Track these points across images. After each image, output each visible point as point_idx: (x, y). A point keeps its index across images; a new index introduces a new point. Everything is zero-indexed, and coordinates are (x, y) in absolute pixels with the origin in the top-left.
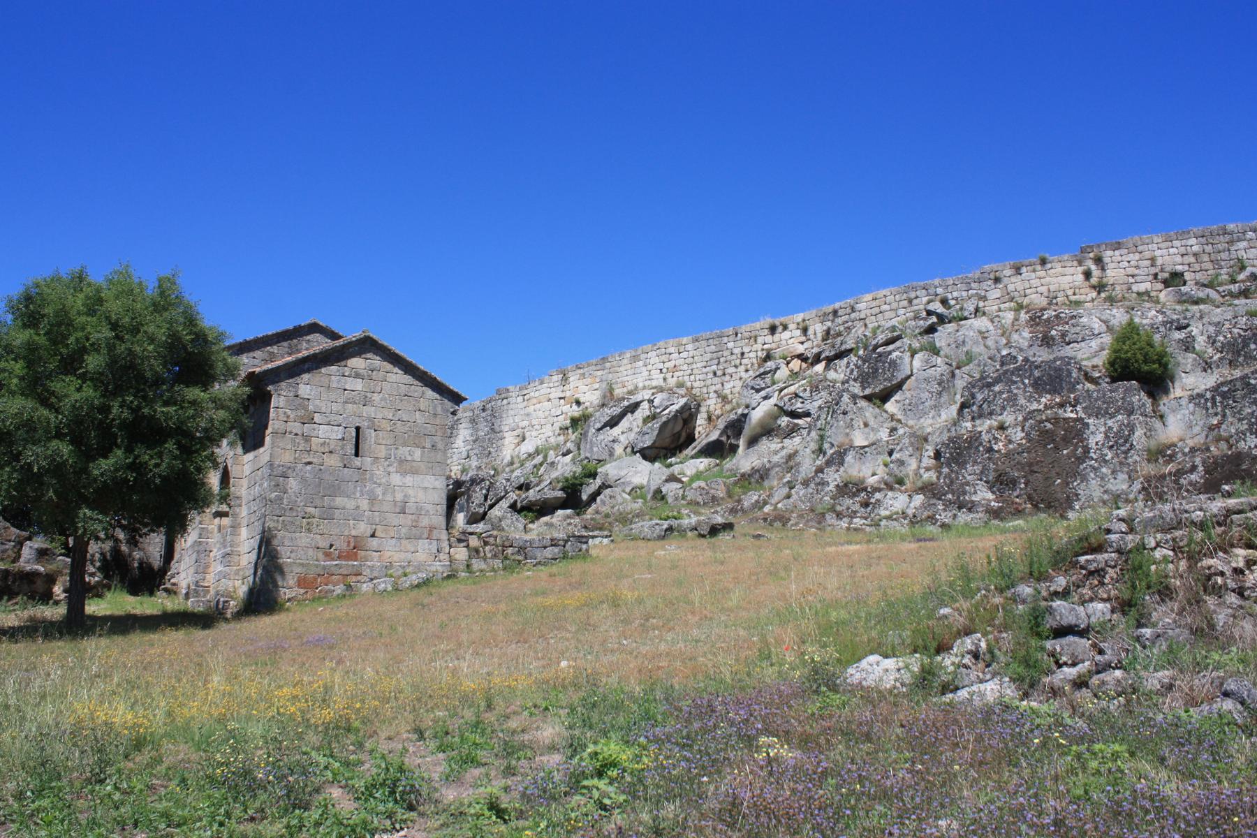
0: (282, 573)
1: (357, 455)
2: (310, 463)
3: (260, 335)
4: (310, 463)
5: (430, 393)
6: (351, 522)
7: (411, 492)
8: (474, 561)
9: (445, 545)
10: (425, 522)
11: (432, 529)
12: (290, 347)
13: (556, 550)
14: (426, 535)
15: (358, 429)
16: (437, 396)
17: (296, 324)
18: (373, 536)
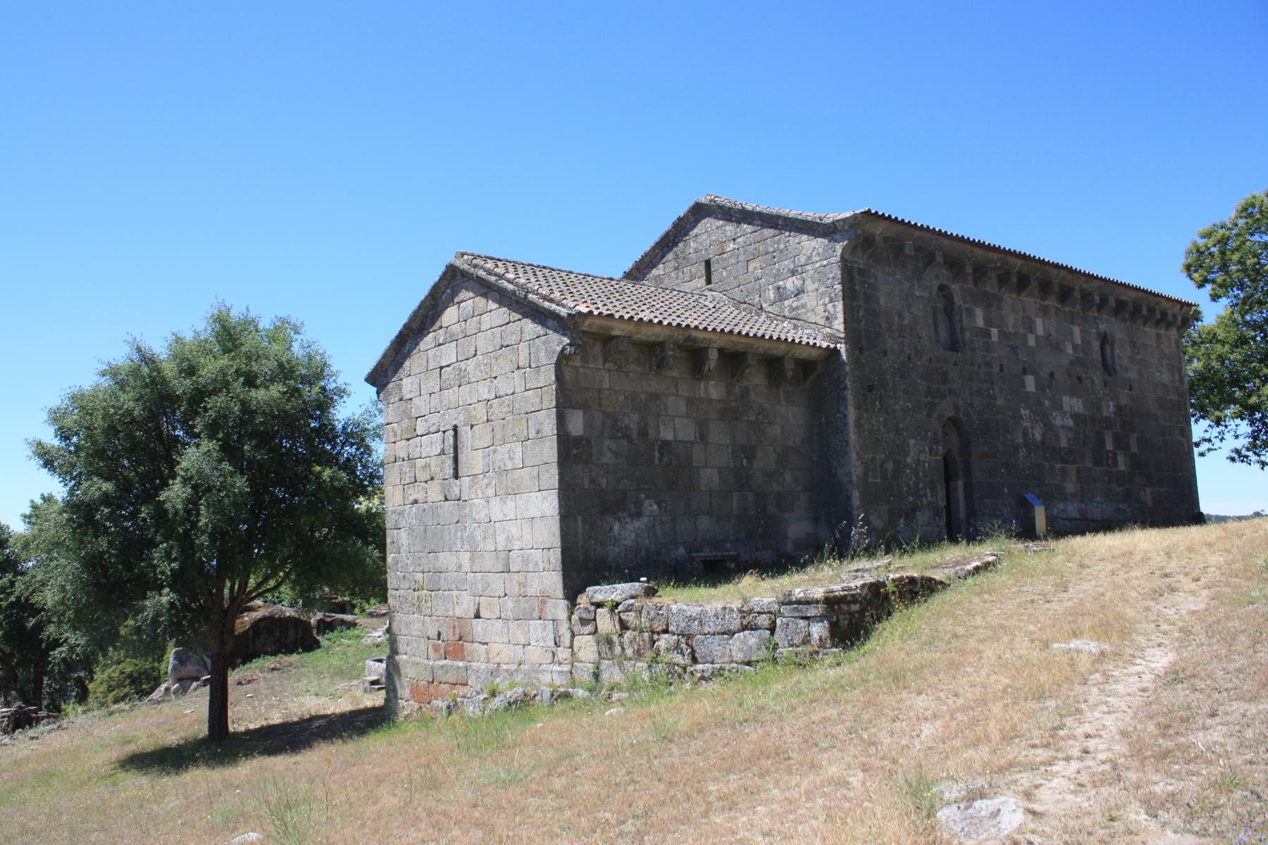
0: (400, 676)
1: (456, 476)
2: (416, 502)
3: (638, 258)
4: (416, 502)
5: (530, 327)
6: (455, 593)
7: (514, 530)
8: (605, 664)
9: (564, 630)
10: (534, 588)
11: (544, 598)
12: (677, 258)
13: (752, 639)
14: (536, 614)
15: (455, 429)
16: (539, 329)
17: (674, 219)
18: (477, 616)
